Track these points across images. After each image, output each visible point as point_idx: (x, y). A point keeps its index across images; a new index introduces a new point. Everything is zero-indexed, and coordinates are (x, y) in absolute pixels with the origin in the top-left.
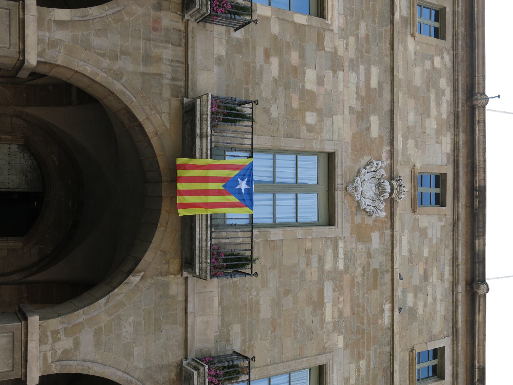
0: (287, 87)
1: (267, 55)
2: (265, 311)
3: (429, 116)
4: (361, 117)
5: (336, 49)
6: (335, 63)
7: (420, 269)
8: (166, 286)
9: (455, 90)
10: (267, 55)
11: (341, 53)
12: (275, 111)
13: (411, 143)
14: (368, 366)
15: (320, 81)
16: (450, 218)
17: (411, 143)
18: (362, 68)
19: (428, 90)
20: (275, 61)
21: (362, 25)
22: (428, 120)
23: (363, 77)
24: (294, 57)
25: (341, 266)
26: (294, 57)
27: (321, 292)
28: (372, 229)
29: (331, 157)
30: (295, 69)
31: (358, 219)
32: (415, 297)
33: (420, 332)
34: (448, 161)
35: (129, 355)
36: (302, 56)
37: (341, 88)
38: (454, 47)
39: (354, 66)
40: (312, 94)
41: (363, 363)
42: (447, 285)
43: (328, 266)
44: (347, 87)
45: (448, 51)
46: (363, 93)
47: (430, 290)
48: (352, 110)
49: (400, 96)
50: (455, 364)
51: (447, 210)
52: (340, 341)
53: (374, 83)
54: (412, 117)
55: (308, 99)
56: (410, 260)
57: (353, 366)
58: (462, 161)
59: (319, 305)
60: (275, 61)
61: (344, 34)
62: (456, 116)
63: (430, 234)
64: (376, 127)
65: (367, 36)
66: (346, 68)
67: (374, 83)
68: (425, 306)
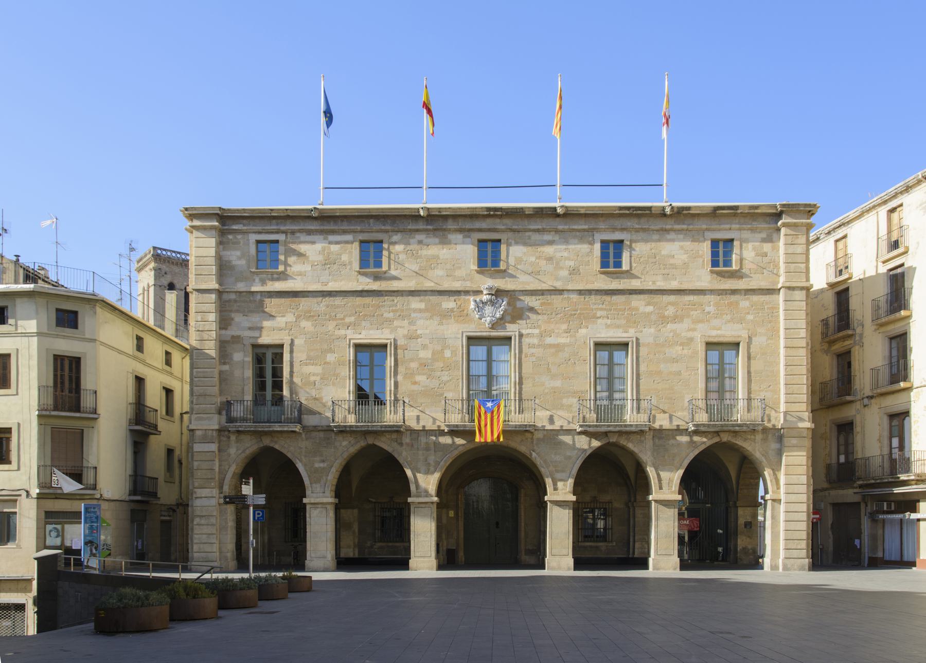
0: (433, 370)
1: (415, 383)
2: (558, 383)
3: (437, 257)
4: (445, 315)
5: (404, 336)
6: (412, 337)
7: (543, 263)
8: (538, 439)
9: (417, 230)
10: (415, 383)
11: (406, 332)
12: (445, 378)
13: (458, 273)
14: (602, 309)
15: (424, 347)
16: (510, 234)
17: (458, 273)
18: (413, 315)
19: (420, 257)
20: (418, 378)
21: (386, 315)
22: (441, 257)
23: (419, 315)
24: (414, 365)
25: (536, 331)
26: (414, 365)
27: (551, 346)
28: (515, 307)
29: (470, 338)
30: (421, 364)
31: (508, 318)
32: (562, 268)
33: (588, 263)
34: (469, 237)
35: (570, 458)
36: (412, 360)
37: (427, 332)
38: (386, 231)
39: (412, 323)
40: (433, 354)
41: (599, 314)
42: (557, 238)
43: (535, 341)
44: (426, 326)
45: (390, 237)
46: (427, 314)
47: (558, 255)
48: (441, 324)
49: (429, 285)
50: (614, 229)
51: (503, 237)
52: (583, 331)
53: (422, 306)
54: (439, 272)
55: (437, 355)
56: (535, 273)
57: (599, 321)
58: (469, 225)
59: (558, 347)
60: (418, 378)
61: (393, 330)
62: (435, 230)
63: (520, 255)
64: (449, 304)
65: (393, 311)
66: (414, 328)
67: (422, 306)
68: (568, 259)
